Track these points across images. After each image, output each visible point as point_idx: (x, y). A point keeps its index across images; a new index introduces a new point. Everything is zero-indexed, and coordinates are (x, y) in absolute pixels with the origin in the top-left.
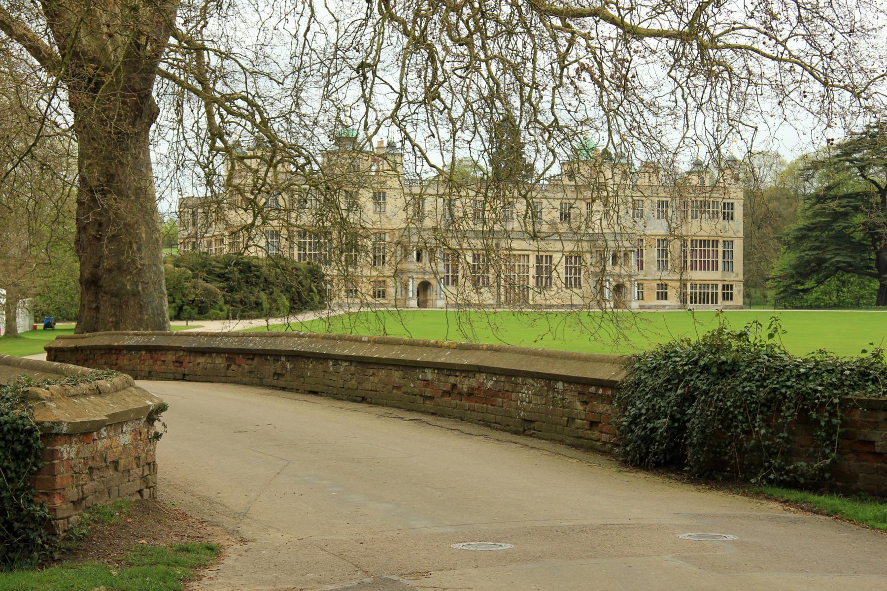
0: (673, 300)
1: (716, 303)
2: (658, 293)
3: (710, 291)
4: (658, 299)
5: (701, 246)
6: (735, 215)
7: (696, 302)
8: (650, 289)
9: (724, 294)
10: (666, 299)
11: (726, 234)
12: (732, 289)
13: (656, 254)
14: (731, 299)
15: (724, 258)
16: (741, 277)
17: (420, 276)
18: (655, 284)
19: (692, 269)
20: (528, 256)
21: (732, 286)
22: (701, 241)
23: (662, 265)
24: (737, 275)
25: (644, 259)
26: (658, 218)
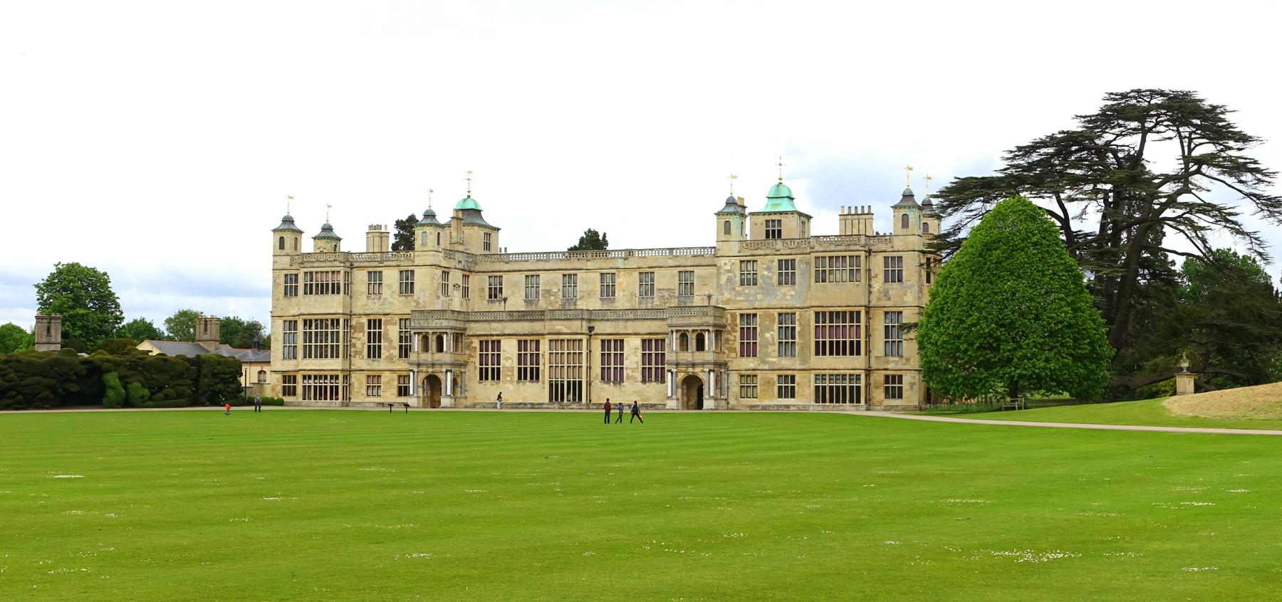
0: (805, 397)
1: (858, 401)
2: (780, 388)
3: (848, 385)
4: (780, 396)
5: (831, 321)
6: (904, 273)
7: (824, 401)
8: (768, 383)
9: (887, 388)
10: (793, 396)
11: (888, 303)
12: (900, 382)
13: (776, 336)
14: (900, 396)
15: (887, 337)
16: (915, 362)
17: (424, 369)
18: (774, 376)
19: (817, 353)
20: (580, 340)
21: (900, 377)
22: (831, 313)
23: (787, 344)
24: (908, 360)
25: (758, 341)
26: (780, 283)
